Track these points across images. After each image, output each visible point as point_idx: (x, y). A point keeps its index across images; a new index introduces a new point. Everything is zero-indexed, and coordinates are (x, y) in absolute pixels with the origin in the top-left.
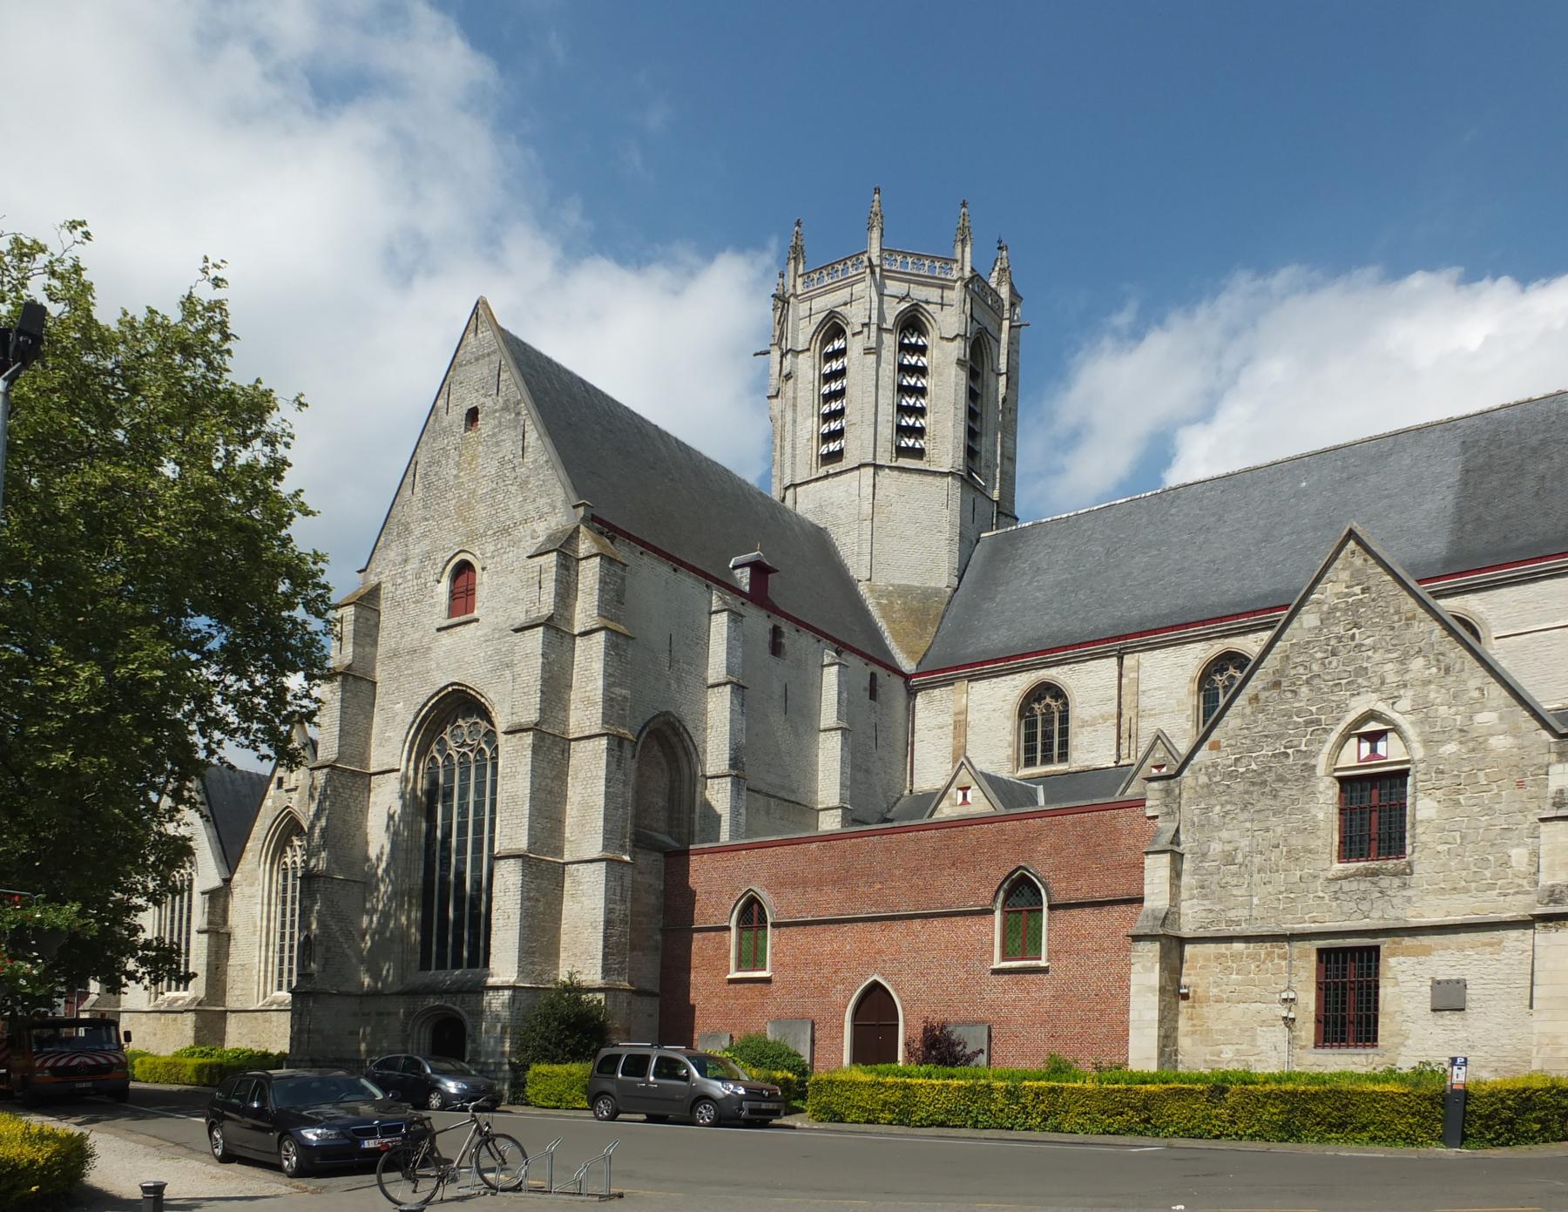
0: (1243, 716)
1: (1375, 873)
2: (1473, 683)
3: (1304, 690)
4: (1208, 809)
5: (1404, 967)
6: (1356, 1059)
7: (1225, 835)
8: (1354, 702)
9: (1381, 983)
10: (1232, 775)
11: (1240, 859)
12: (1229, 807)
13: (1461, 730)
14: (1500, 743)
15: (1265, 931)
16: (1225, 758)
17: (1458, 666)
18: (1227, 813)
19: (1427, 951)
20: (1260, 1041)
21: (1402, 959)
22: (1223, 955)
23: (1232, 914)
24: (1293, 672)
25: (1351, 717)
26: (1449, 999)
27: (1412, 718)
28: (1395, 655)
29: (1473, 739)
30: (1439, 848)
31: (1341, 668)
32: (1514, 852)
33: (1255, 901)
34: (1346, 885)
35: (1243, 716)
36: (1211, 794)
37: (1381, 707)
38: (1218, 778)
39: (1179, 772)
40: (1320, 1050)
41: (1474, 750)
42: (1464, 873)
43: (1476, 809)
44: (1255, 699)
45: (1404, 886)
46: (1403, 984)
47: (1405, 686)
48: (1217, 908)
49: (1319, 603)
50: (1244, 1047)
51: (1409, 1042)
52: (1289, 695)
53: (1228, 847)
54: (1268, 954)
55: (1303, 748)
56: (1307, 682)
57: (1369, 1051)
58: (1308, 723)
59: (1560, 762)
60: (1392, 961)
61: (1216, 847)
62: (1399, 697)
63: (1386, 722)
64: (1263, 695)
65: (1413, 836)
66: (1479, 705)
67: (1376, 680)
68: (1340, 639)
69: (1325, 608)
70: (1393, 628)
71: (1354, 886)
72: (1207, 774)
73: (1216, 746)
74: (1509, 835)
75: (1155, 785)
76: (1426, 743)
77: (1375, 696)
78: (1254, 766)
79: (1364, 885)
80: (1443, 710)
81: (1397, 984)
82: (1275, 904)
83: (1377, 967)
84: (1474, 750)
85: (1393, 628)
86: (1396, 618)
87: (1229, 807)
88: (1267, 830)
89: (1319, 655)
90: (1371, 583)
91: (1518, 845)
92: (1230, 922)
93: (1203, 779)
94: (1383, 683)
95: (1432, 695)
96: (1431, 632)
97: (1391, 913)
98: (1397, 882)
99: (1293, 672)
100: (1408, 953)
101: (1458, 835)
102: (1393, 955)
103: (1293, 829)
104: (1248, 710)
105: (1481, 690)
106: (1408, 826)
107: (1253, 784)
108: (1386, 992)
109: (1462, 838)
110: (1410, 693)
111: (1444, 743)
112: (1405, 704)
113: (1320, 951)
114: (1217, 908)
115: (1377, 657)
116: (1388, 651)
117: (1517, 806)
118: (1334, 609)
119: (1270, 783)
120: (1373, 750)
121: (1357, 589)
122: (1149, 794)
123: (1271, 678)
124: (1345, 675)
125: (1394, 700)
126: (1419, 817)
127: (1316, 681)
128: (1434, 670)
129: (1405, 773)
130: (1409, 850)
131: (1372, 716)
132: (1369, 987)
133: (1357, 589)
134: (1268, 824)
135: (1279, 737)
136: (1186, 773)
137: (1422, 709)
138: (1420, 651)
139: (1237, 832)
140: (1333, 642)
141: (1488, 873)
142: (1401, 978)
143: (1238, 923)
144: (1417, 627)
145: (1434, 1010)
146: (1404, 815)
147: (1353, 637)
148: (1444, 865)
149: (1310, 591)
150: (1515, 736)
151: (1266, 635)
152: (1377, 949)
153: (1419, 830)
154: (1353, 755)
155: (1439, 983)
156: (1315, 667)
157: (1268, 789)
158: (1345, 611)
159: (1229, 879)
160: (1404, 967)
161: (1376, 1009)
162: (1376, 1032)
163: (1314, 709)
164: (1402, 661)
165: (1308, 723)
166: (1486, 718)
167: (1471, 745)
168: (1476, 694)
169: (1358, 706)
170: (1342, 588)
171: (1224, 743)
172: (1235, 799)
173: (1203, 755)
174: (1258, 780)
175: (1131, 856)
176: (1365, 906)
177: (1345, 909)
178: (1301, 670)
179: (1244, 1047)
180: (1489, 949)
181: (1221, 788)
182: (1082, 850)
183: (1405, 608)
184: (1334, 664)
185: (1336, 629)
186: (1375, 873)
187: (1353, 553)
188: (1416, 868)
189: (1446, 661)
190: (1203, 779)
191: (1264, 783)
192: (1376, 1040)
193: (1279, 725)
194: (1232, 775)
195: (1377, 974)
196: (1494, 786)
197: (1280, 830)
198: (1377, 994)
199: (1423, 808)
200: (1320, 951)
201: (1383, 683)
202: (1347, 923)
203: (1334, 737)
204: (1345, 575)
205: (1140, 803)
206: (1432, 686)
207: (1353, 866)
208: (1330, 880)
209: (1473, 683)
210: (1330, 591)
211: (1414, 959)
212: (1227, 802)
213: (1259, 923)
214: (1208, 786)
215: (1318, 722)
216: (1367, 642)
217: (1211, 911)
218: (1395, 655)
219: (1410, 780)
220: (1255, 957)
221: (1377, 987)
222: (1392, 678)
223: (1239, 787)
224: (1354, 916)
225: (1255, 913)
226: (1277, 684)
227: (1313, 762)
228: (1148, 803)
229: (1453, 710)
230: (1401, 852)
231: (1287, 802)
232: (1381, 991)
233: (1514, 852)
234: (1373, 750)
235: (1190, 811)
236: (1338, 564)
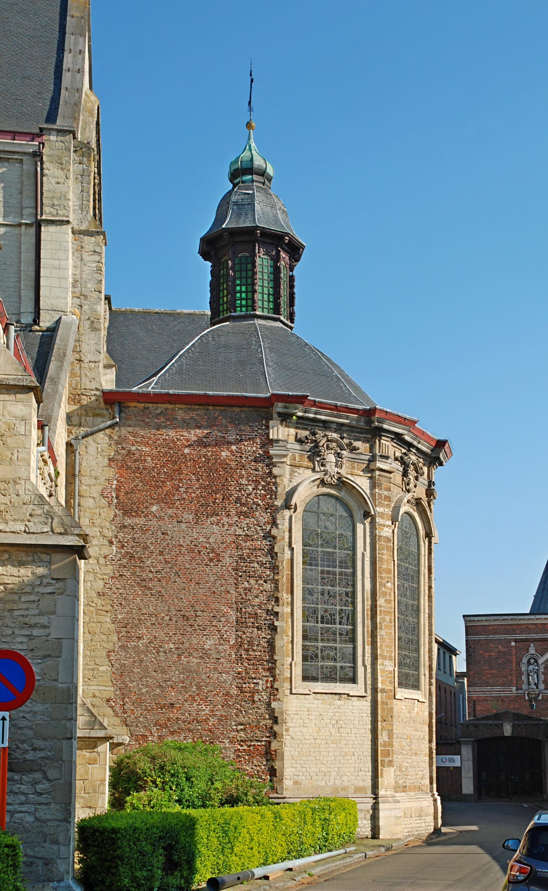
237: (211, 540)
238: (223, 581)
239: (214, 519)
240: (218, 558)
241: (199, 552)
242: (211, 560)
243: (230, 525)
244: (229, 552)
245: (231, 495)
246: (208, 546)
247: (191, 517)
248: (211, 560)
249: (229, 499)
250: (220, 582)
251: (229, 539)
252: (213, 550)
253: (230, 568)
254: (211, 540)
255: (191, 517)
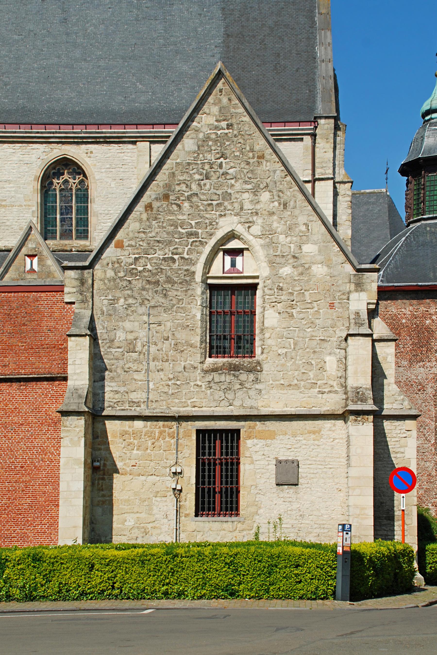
0: (141, 220)
1: (235, 368)
2: (302, 219)
3: (186, 205)
4: (115, 300)
5: (257, 448)
6: (225, 525)
7: (128, 325)
8: (222, 221)
9: (242, 460)
10: (132, 272)
11: (139, 348)
12: (130, 301)
13: (294, 257)
14: (319, 270)
15: (157, 412)
16: (126, 256)
17: (292, 203)
18: (129, 306)
19: (272, 436)
20: (155, 510)
21: (255, 441)
22: (126, 433)
23: (133, 396)
24: (177, 188)
25: (220, 234)
26: (288, 476)
27: (261, 241)
28: (250, 187)
29: (302, 265)
30: (280, 351)
31: (212, 190)
32: (328, 359)
33: (151, 385)
34: (217, 377)
35: (141, 220)
36: (116, 287)
37: (240, 229)
38: (122, 274)
39: (91, 266)
40: (199, 518)
41: (302, 274)
42: (296, 373)
43: (304, 322)
44: (149, 207)
45: (257, 380)
46: (257, 460)
47: (257, 214)
48: (122, 389)
49: (197, 131)
50: (143, 515)
51: (261, 511)
52: (175, 207)
53: (130, 337)
54: (161, 433)
55: (186, 256)
56: (189, 198)
57: (234, 518)
58: (190, 234)
59: (356, 291)
60: (249, 442)
61: (120, 336)
62: (253, 222)
63: (245, 243)
64: (156, 205)
65: (263, 340)
66: (304, 238)
67: (236, 205)
68: (211, 165)
69: (201, 136)
70: (248, 163)
71: (223, 378)
72: (114, 269)
73: (120, 245)
74: (325, 345)
75: (72, 274)
76: (271, 263)
77: (236, 219)
78: (149, 267)
79: (229, 378)
80: (282, 238)
81: (252, 463)
82: (166, 389)
83: (238, 447)
84: (302, 274)
85: (248, 163)
86: (251, 155)
87: (130, 301)
88: (160, 324)
89: (197, 177)
90: (234, 121)
91: (330, 354)
92: (132, 403)
93: (110, 273)
94: (242, 209)
95: (275, 225)
96: (275, 171)
97: (248, 403)
98: (252, 377)
99: (177, 188)
100: (261, 436)
101: (292, 341)
102: (250, 438)
103: (178, 325)
104: (144, 216)
105: (307, 225)
106: (257, 331)
107: (149, 282)
108: (245, 468)
109: (295, 344)
110: (259, 221)
111: (284, 265)
112: (256, 229)
113: (198, 432)
114: (122, 389)
115: (238, 186)
116: (246, 182)
117: (330, 322)
118: (207, 138)
119: (159, 283)
120: (233, 264)
121: (224, 124)
122: (67, 282)
123: (161, 191)
124: (215, 197)
125: (249, 224)
126: (266, 325)
127: (195, 199)
128: (276, 204)
129: (254, 287)
130: (258, 351)
131: (232, 236)
132: (232, 464)
133: (224, 124)
134: (160, 319)
135: (170, 243)
136: (97, 267)
137: (268, 234)
138: (267, 186)
139: (136, 324)
140: (207, 167)
141: (311, 374)
142: (255, 457)
143: (138, 404)
144: (266, 166)
145: (277, 485)
146: (253, 322)
147: (221, 166)
148: (283, 365)
149: (191, 119)
150: (328, 266)
151: (159, 150)
152: (238, 431)
153: (267, 335)
154: (220, 267)
155: (280, 462)
156: (194, 187)
157: (160, 288)
158: (215, 141)
159: (130, 365)
160: (257, 448)
161: (238, 482)
162: (238, 502)
163: (193, 223)
164: (255, 192)
165: (190, 234)
166: (309, 249)
167: (301, 269)
168: (303, 228)
169: (225, 226)
170: (211, 120)
171: (126, 244)
172: (136, 294)
173: (110, 252)
174: (152, 279)
175: (52, 338)
176: (230, 396)
177: (216, 397)
178: (183, 187)
179: (143, 515)
180: (313, 436)
181: (125, 283)
182: (9, 328)
183: (257, 148)
184: (208, 186)
185: (209, 156)
186: (235, 368)
187: (221, 91)
188: (265, 367)
189: (285, 198)
190: (110, 273)
191: (157, 283)
192: (237, 509)
193: (168, 233)
194: (132, 272)
195: (238, 453)
196: (315, 304)
197: (169, 324)
198: (238, 470)
199: (268, 317)
200: (198, 432)
201: (242, 209)
202: (218, 409)
203: (207, 249)
204: (215, 110)
205: (59, 289)
206: (275, 217)
207: (221, 361)
208: (206, 372)
209: (302, 219)
210: (205, 121)
211: (263, 442)
212: (129, 296)
213: (154, 405)
214: (114, 280)
215: (196, 234)
216: (231, 171)
217: (117, 392)
218: (250, 187)
219: (259, 293)
220: (150, 434)
221: (238, 463)
222: (247, 206)
223: (138, 284)
224: (223, 403)
225: (151, 397)
226: (166, 197)
227: (193, 269)
228: (66, 290)
229: (289, 239)
230: (252, 353)
231: (174, 302)
232: (242, 467)
233: (328, 359)
234: (233, 264)
235: (101, 302)
236: (211, 99)
237: (419, 378)
238: (427, 404)
239: (421, 364)
240: (423, 389)
241: (412, 385)
242: (419, 390)
243: (432, 367)
244: (430, 385)
245: (432, 348)
246: (417, 381)
247: (406, 363)
248: (419, 390)
249: (430, 351)
250: (424, 404)
251: (431, 376)
252: (420, 384)
253: (431, 395)
254: (419, 378)
255: (406, 363)
